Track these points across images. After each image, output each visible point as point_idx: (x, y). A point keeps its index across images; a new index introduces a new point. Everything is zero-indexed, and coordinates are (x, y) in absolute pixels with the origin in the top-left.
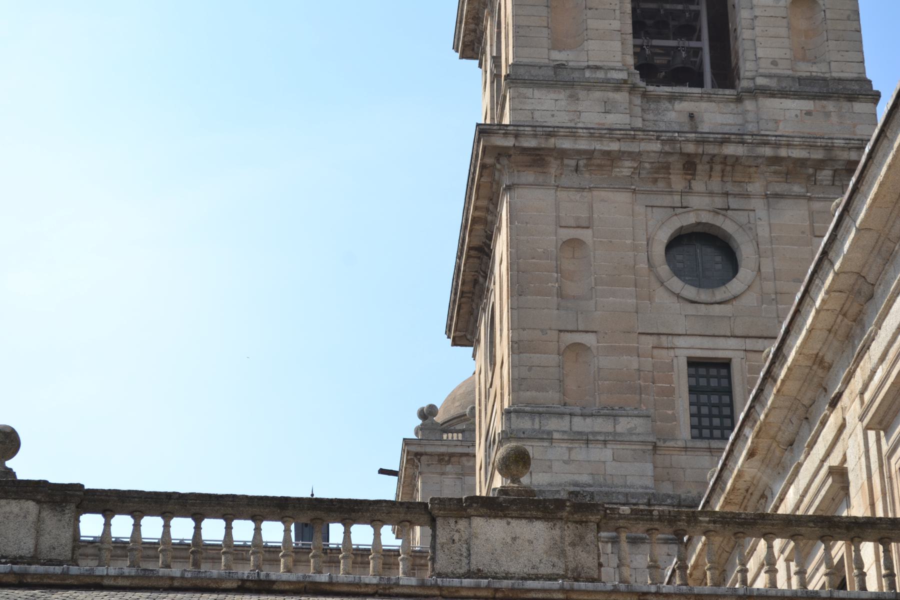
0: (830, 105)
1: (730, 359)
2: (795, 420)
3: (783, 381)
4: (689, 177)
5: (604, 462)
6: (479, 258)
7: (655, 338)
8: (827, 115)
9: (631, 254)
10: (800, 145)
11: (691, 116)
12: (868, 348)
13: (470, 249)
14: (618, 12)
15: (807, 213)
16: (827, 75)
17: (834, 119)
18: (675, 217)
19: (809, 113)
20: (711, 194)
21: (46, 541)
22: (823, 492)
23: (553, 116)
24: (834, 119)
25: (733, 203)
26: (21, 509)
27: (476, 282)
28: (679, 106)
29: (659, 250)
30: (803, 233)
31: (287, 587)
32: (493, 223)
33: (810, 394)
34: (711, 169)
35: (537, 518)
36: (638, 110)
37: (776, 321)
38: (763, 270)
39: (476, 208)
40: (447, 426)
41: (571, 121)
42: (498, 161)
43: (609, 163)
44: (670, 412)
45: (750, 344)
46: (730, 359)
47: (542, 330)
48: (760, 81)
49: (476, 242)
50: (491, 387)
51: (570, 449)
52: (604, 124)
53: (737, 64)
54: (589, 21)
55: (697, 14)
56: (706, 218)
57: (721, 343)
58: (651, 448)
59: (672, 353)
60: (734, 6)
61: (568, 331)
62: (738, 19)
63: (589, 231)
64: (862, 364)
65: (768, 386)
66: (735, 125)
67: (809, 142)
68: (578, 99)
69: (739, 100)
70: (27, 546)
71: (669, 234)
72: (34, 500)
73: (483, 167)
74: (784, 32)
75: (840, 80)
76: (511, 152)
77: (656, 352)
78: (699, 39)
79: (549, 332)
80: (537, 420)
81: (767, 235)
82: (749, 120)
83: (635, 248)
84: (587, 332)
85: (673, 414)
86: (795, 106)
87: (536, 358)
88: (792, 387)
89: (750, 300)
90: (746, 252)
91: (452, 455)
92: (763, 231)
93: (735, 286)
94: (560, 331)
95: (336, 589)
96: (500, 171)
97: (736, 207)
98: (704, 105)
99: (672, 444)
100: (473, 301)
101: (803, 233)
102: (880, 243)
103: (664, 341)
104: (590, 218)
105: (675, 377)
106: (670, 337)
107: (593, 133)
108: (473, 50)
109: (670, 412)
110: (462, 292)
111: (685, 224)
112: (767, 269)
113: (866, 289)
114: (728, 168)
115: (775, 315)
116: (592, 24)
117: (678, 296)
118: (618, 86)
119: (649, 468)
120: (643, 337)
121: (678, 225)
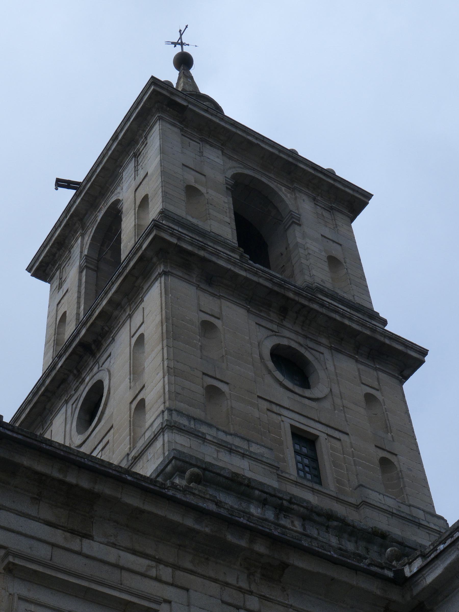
10: (357, 322)
18: (275, 337)
20: (297, 333)
44: (282, 456)
51: (218, 451)
56: (294, 345)
59: (279, 418)
71: (272, 345)
77: (269, 413)
79: (195, 370)
89: (327, 404)
92: (330, 367)
94: (204, 374)
99: (287, 476)
103: (275, 408)
112: (336, 390)
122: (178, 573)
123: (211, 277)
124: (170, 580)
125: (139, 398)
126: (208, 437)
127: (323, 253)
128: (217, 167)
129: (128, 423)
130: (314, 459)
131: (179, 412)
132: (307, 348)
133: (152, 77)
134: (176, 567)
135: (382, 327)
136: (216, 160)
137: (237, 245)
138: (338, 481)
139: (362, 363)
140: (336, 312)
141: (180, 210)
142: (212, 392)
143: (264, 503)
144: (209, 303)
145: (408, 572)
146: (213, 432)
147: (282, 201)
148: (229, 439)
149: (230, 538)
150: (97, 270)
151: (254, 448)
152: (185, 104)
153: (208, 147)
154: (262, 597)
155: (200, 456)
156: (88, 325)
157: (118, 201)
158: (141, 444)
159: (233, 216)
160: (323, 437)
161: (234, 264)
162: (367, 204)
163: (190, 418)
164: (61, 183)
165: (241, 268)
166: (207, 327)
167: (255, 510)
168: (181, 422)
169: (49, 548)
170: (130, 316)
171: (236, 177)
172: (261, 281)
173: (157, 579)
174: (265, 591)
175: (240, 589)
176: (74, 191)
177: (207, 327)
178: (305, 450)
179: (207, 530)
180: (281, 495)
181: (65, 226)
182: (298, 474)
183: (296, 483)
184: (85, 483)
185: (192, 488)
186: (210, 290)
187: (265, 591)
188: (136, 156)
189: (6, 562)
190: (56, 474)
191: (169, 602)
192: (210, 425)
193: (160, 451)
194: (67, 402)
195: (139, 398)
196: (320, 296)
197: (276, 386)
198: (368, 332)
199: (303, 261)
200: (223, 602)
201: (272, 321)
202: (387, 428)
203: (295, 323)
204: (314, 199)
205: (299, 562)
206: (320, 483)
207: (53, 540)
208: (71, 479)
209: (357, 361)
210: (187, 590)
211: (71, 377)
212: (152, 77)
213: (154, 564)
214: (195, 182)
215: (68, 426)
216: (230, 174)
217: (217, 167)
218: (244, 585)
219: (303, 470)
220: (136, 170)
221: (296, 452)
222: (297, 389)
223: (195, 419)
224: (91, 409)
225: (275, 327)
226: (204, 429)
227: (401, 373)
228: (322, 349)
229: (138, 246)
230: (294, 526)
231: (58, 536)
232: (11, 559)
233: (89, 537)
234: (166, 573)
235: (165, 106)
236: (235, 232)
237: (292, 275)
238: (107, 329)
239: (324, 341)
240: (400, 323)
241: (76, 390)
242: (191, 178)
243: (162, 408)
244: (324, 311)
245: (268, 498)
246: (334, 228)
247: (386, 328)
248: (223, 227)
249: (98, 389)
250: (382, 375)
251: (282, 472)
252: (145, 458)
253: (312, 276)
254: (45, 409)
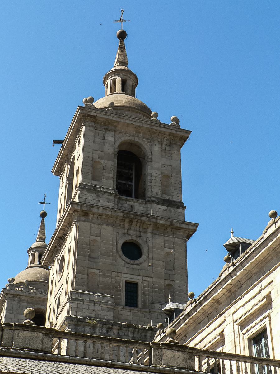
0: (172, 209)
1: (138, 282)
2: (204, 317)
3: (205, 306)
4: (130, 225)
5: (99, 311)
6: (59, 240)
7: (116, 273)
8: (171, 212)
9: (111, 246)
11: (132, 206)
12: (238, 302)
13: (57, 237)
14: (113, 172)
15: (163, 241)
16: (171, 200)
17: (173, 213)
19: (166, 210)
21: (45, 345)
22: (215, 340)
23: (91, 201)
24: (173, 213)
25: (142, 234)
26: (38, 335)
27: (56, 247)
28: (128, 203)
29: (120, 247)
30: (162, 246)
31: (119, 367)
32: (67, 231)
33: (211, 310)
34: (137, 223)
35: (180, 351)
36: (116, 203)
37: (152, 272)
38: (149, 256)
39: (63, 225)
40: (17, 285)
41: (97, 203)
42: (74, 213)
43: (107, 218)
45: (144, 278)
46: (138, 282)
47: (83, 267)
48: (153, 199)
49: (60, 235)
50: (59, 282)
51: (89, 305)
52: (106, 205)
53: (144, 192)
54: (104, 173)
55: (131, 174)
56: (134, 238)
58: (113, 307)
60: (145, 175)
61: (91, 268)
62: (147, 179)
64: (234, 305)
65: (198, 306)
66: (144, 211)
67: (166, 219)
68: (99, 197)
69: (146, 203)
70: (39, 346)
72: (41, 333)
73: (69, 214)
74: (160, 185)
75: (175, 202)
76: (79, 210)
77: (116, 278)
78: (131, 181)
80: (80, 295)
81: (151, 245)
82: (148, 210)
83: (113, 245)
84: (97, 269)
85: (120, 298)
86: (162, 207)
87: (81, 276)
88: (206, 308)
89: (145, 265)
90: (145, 250)
91: (18, 295)
92: (150, 244)
93: (141, 260)
94: (89, 268)
95: (132, 368)
96: (74, 215)
97: (143, 236)
98: (136, 204)
100: (53, 253)
101: (162, 246)
102: (248, 274)
104: (100, 234)
106: (121, 274)
107: (104, 208)
108: (58, 173)
109: (119, 297)
110: (51, 250)
111: (128, 239)
112: (150, 256)
113: (240, 285)
115: (152, 270)
116: (105, 174)
117: (124, 261)
118: (111, 194)
119: (112, 313)
120: (113, 273)
121: (126, 239)
147: (145, 148)
152: (95, 114)
181: (61, 158)
214: (99, 158)
235: (87, 117)
246: (170, 156)
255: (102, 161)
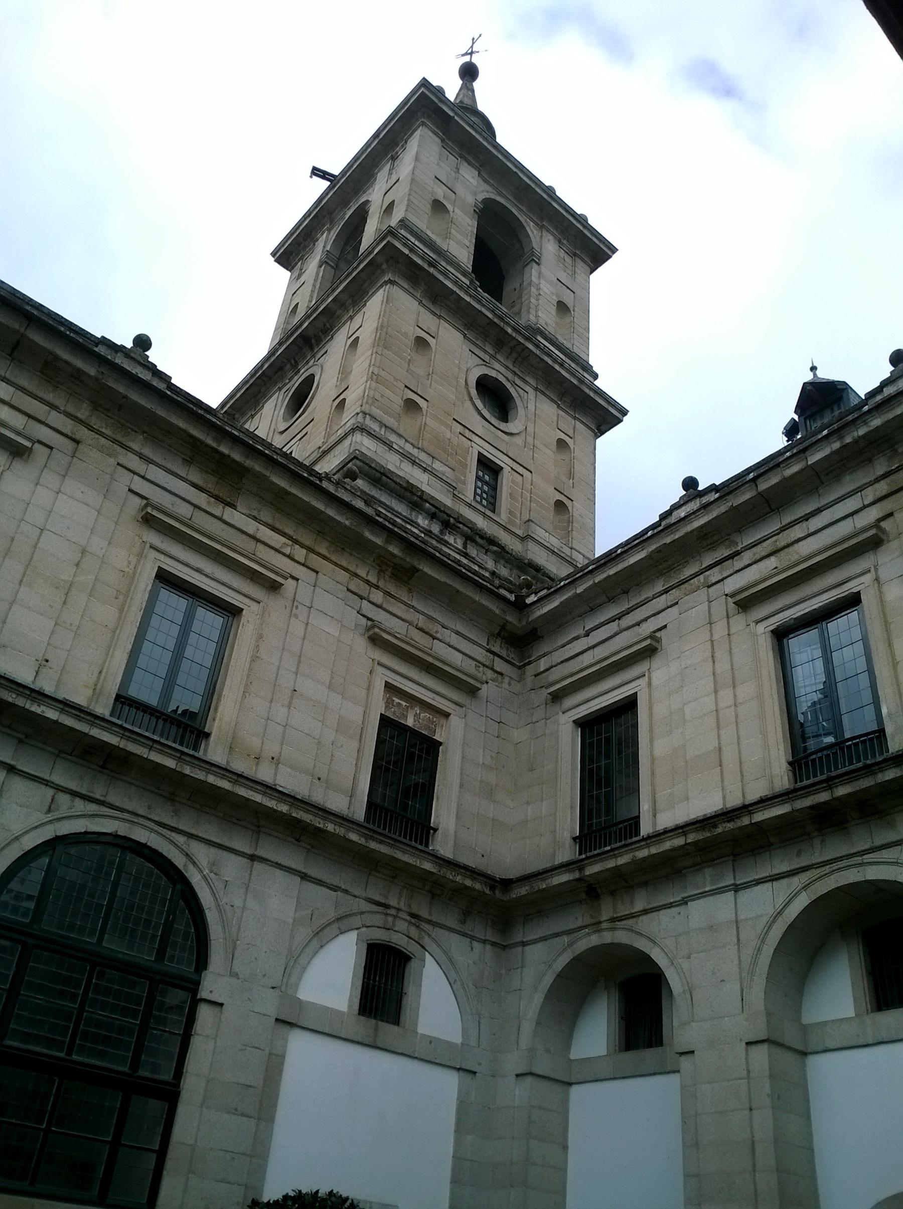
13: (300, 335)
20: (507, 367)
27: (281, 368)
51: (401, 461)
56: (501, 379)
57: (500, 455)
63: (434, 341)
89: (518, 440)
92: (531, 407)
93: (511, 427)
94: (406, 386)
99: (463, 497)
103: (467, 433)
105: (469, 459)
112: (530, 429)
114: (520, 359)
122: (312, 555)
123: (437, 296)
124: (303, 561)
125: (341, 397)
126: (395, 446)
127: (554, 297)
128: (471, 187)
129: (326, 419)
130: (494, 488)
131: (373, 418)
132: (514, 384)
133: (424, 78)
134: (310, 550)
135: (592, 379)
136: (472, 180)
137: (470, 271)
138: (511, 512)
139: (563, 410)
140: (549, 356)
141: (421, 222)
142: (411, 406)
143: (433, 516)
144: (429, 321)
145: (529, 600)
146: (401, 442)
148: (415, 452)
149: (368, 535)
150: (336, 268)
151: (437, 465)
152: (451, 114)
153: (466, 164)
154: (387, 593)
155: (383, 463)
156: (312, 318)
157: (367, 202)
158: (333, 439)
159: (474, 241)
160: (507, 470)
161: (461, 287)
162: (610, 257)
163: (382, 425)
164: (317, 172)
165: (467, 293)
166: (421, 343)
167: (423, 521)
168: (372, 426)
169: (191, 508)
170: (351, 318)
171: (486, 201)
172: (484, 310)
173: (289, 557)
174: (392, 589)
175: (368, 582)
176: (328, 183)
177: (421, 343)
178: (487, 478)
179: (347, 523)
180: (449, 512)
182: (475, 497)
183: (470, 506)
184: (237, 457)
185: (345, 483)
186: (432, 308)
187: (392, 589)
188: (394, 159)
189: (144, 512)
190: (210, 441)
191: (297, 580)
192: (400, 436)
193: (347, 450)
194: (280, 389)
195: (341, 397)
196: (539, 338)
197: (473, 414)
198: (575, 382)
199: (533, 300)
200: (348, 590)
201: (485, 351)
202: (571, 475)
203: (507, 358)
204: (560, 242)
205: (427, 569)
206: (494, 511)
207: (196, 502)
208: (224, 449)
209: (558, 406)
210: (317, 572)
211: (288, 366)
212: (424, 78)
213: (290, 543)
215: (276, 412)
216: (481, 197)
217: (471, 187)
218: (373, 580)
219: (481, 496)
220: (390, 174)
221: (478, 478)
222: (494, 421)
223: (386, 427)
224: (300, 399)
225: (487, 358)
226: (393, 438)
227: (598, 428)
228: (527, 388)
229: (370, 249)
230: (455, 542)
231: (202, 499)
232: (149, 510)
233: (233, 506)
234: (300, 553)
236: (472, 257)
237: (519, 313)
238: (328, 325)
239: (532, 381)
240: (610, 381)
241: (291, 379)
242: (440, 193)
243: (358, 410)
244: (537, 352)
245: (438, 513)
247: (595, 383)
248: (461, 249)
249: (309, 381)
250: (579, 425)
251: (459, 493)
252: (332, 453)
253: (537, 316)
254: (260, 392)
255: (449, 207)
